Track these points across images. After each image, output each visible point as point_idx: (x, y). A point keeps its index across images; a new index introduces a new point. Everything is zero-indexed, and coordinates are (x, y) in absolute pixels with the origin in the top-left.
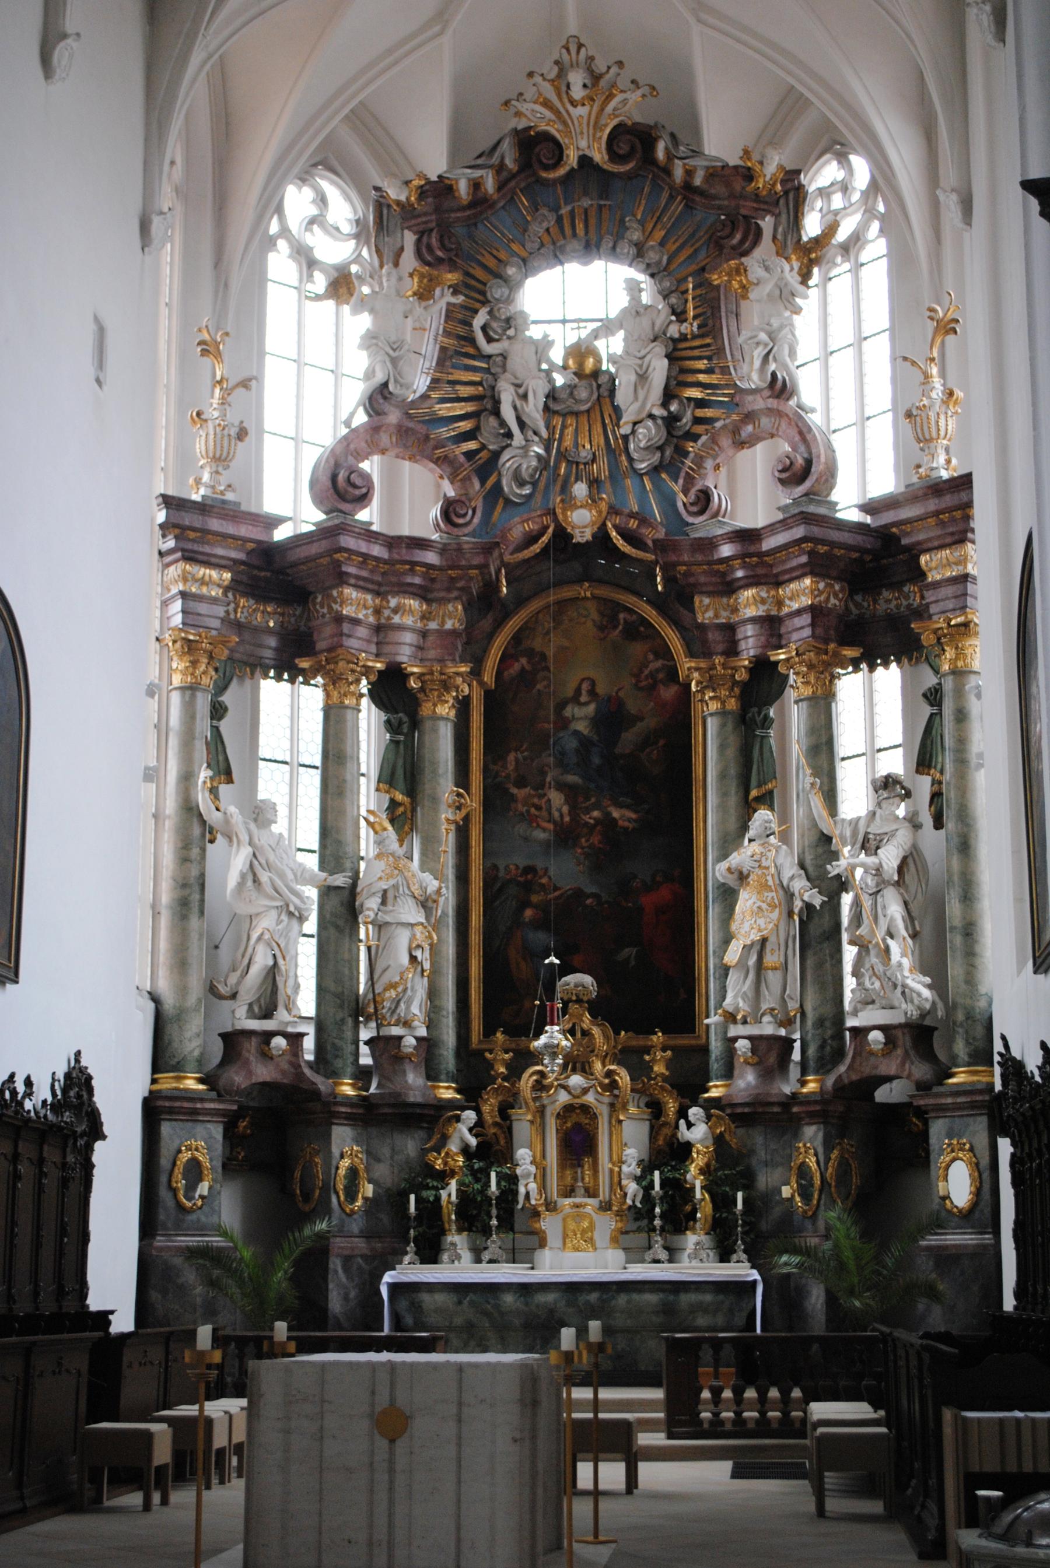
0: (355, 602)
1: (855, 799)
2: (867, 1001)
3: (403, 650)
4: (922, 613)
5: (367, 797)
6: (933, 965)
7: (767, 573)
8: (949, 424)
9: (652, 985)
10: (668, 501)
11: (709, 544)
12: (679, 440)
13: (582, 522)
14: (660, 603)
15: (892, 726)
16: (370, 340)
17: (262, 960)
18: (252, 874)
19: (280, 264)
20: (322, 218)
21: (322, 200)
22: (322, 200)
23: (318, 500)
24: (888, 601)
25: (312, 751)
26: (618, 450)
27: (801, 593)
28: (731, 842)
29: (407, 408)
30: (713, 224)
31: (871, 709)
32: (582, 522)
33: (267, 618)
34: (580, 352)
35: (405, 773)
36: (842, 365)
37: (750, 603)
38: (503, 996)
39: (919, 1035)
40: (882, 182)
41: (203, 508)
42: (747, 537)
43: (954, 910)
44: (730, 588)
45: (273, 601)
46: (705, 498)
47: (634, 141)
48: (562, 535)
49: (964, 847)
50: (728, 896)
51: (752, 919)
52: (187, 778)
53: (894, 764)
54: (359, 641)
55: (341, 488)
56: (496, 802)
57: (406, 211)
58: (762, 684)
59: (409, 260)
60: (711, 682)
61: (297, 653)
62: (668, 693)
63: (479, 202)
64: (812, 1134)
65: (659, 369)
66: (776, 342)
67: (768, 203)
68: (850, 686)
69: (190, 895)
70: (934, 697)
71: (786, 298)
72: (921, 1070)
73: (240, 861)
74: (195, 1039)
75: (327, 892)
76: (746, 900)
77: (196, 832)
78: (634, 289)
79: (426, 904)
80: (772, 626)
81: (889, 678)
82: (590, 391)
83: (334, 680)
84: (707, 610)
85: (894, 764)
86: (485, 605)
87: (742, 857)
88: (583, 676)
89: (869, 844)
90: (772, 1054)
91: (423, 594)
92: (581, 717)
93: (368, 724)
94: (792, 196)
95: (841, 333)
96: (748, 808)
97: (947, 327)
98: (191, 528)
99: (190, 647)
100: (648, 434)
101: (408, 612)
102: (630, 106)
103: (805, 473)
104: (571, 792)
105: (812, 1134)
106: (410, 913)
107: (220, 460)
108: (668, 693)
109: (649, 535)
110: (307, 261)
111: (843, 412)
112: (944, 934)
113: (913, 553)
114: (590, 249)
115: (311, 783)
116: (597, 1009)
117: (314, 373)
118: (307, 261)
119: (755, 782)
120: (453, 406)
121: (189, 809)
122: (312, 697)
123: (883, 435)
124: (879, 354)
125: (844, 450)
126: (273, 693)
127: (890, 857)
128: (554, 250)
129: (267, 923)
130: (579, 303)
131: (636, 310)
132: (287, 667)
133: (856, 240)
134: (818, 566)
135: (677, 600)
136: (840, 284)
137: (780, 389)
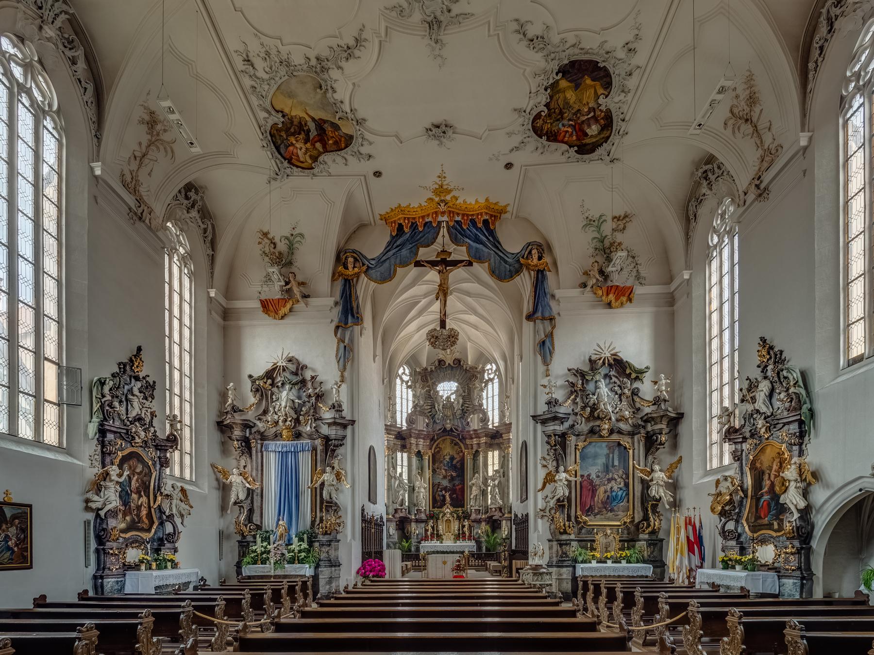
0: (413, 441)
1: (490, 473)
2: (492, 503)
3: (420, 448)
4: (502, 443)
5: (415, 471)
6: (502, 498)
7: (478, 437)
8: (508, 414)
9: (459, 501)
10: (462, 423)
11: (469, 431)
12: (464, 413)
13: (448, 426)
14: (460, 440)
15: (496, 461)
16: (414, 396)
17: (401, 498)
18: (399, 485)
19: (398, 381)
20: (404, 372)
21: (404, 369)
22: (404, 369)
23: (407, 422)
24: (497, 441)
25: (405, 463)
26: (454, 414)
27: (483, 440)
28: (471, 479)
29: (421, 407)
30: (469, 376)
31: (493, 459)
32: (448, 426)
33: (399, 443)
34: (448, 398)
35: (422, 468)
36: (490, 400)
37: (475, 441)
38: (437, 502)
39: (500, 509)
40: (498, 369)
41: (390, 426)
42: (475, 430)
43: (506, 490)
44: (472, 438)
45: (401, 439)
46: (468, 424)
47: (458, 362)
48: (445, 428)
49: (508, 481)
50: (471, 488)
51: (475, 491)
52: (389, 469)
53: (496, 467)
54: (414, 447)
55: (410, 420)
56: (434, 471)
57: (420, 373)
58: (476, 454)
59: (420, 380)
60: (469, 453)
61: (403, 448)
62: (461, 454)
63: (432, 371)
64: (483, 523)
65: (461, 401)
66: (481, 397)
67: (479, 372)
68: (490, 454)
69: (389, 488)
70: (504, 457)
71: (482, 390)
72: (500, 514)
73: (397, 483)
74: (391, 511)
75: (409, 487)
76: (474, 488)
77: (390, 478)
78: (457, 387)
79: (425, 488)
80: (478, 444)
81: (496, 453)
82: (449, 405)
83: (409, 453)
84: (468, 442)
85: (496, 467)
86: (433, 440)
87: (473, 481)
88: (448, 450)
89: (494, 480)
90: (478, 512)
91: (424, 439)
92: (447, 458)
93: (414, 459)
94: (483, 371)
95: (490, 395)
96: (474, 474)
97: (508, 397)
98: (388, 429)
99: (388, 448)
100: (459, 412)
101: (421, 442)
102: (457, 355)
103: (485, 420)
104: (446, 470)
105: (483, 523)
106: (423, 490)
107: (392, 417)
108: (461, 454)
109: (460, 429)
110: (402, 381)
111: (490, 409)
112: (504, 494)
113: (501, 434)
114: (449, 380)
115: (405, 469)
116: (451, 505)
117: (405, 400)
118: (402, 381)
119: (475, 470)
120: (427, 403)
121: (389, 474)
122: (405, 455)
123: (496, 412)
124: (496, 399)
125: (490, 414)
126: (399, 454)
127: (496, 482)
128: (443, 380)
129: (401, 492)
130: (447, 389)
131: (456, 392)
132: (402, 451)
133: (493, 378)
134: (486, 436)
135: (463, 440)
136: (490, 386)
137: (481, 405)
